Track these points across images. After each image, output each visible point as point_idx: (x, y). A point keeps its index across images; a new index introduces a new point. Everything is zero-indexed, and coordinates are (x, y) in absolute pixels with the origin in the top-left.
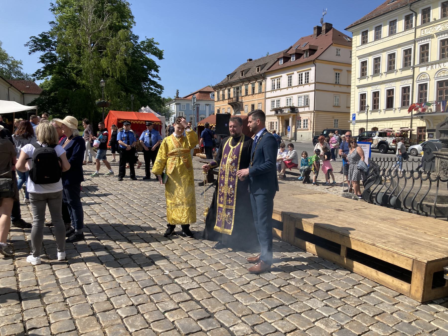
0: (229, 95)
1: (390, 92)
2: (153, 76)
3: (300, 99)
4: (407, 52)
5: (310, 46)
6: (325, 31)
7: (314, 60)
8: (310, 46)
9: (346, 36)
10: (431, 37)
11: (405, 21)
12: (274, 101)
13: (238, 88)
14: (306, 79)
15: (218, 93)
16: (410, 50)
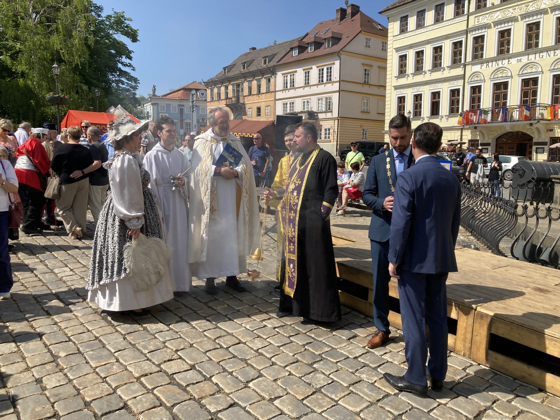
0: (227, 93)
1: (436, 95)
2: (125, 65)
3: (320, 101)
4: (457, 45)
5: (332, 32)
6: (350, 15)
7: (339, 52)
8: (332, 32)
10: (487, 26)
11: (455, 5)
13: (238, 85)
14: (327, 76)
15: (212, 91)
16: (461, 42)
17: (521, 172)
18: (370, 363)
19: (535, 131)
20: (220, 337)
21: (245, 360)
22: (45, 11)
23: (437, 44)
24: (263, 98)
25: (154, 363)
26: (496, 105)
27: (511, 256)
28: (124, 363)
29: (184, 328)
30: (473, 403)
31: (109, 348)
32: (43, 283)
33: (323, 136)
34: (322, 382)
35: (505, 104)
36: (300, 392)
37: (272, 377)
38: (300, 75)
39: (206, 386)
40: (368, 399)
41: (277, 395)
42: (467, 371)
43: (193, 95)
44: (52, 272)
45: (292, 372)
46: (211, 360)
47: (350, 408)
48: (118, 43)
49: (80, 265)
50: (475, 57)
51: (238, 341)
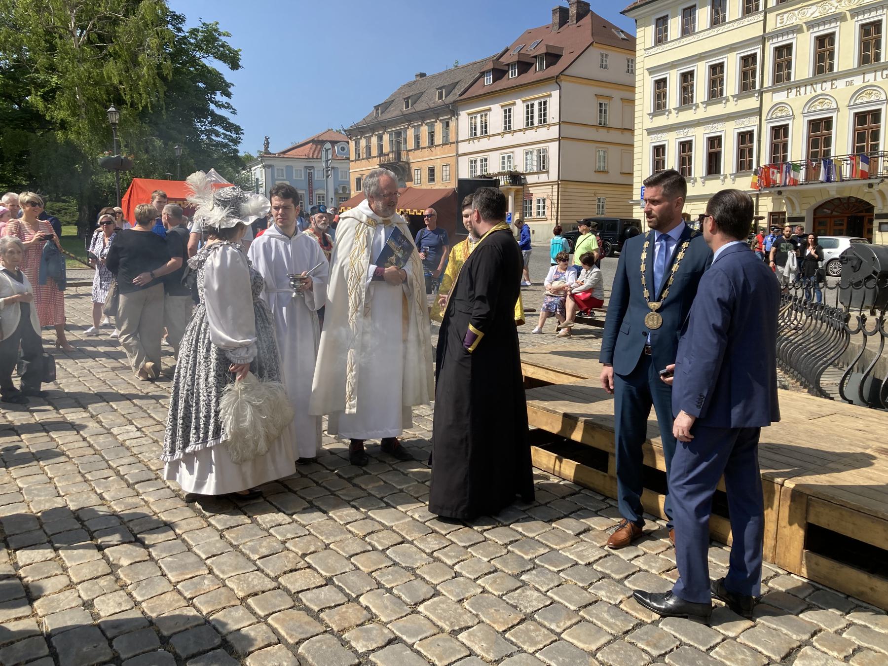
0: (381, 147)
1: (714, 142)
3: (529, 156)
4: (748, 61)
5: (547, 46)
6: (575, 17)
8: (547, 46)
9: (616, 28)
10: (796, 30)
12: (475, 161)
13: (398, 134)
14: (540, 116)
15: (357, 144)
16: (754, 56)
17: (855, 263)
18: (612, 572)
19: (878, 196)
20: (373, 532)
21: (413, 569)
22: (94, 24)
23: (716, 61)
24: (438, 152)
25: (267, 575)
26: (812, 156)
27: (840, 399)
28: (221, 576)
29: (315, 519)
30: (779, 635)
31: (197, 551)
32: (95, 450)
33: (534, 211)
34: (534, 603)
35: (827, 153)
36: (499, 620)
37: (454, 596)
38: (495, 114)
39: (350, 610)
40: (609, 630)
41: (463, 625)
42: (770, 584)
43: (327, 150)
44: (109, 432)
45: (487, 587)
46: (359, 569)
47: (581, 645)
48: (210, 71)
49: (151, 422)
50: (777, 79)
51: (400, 540)
